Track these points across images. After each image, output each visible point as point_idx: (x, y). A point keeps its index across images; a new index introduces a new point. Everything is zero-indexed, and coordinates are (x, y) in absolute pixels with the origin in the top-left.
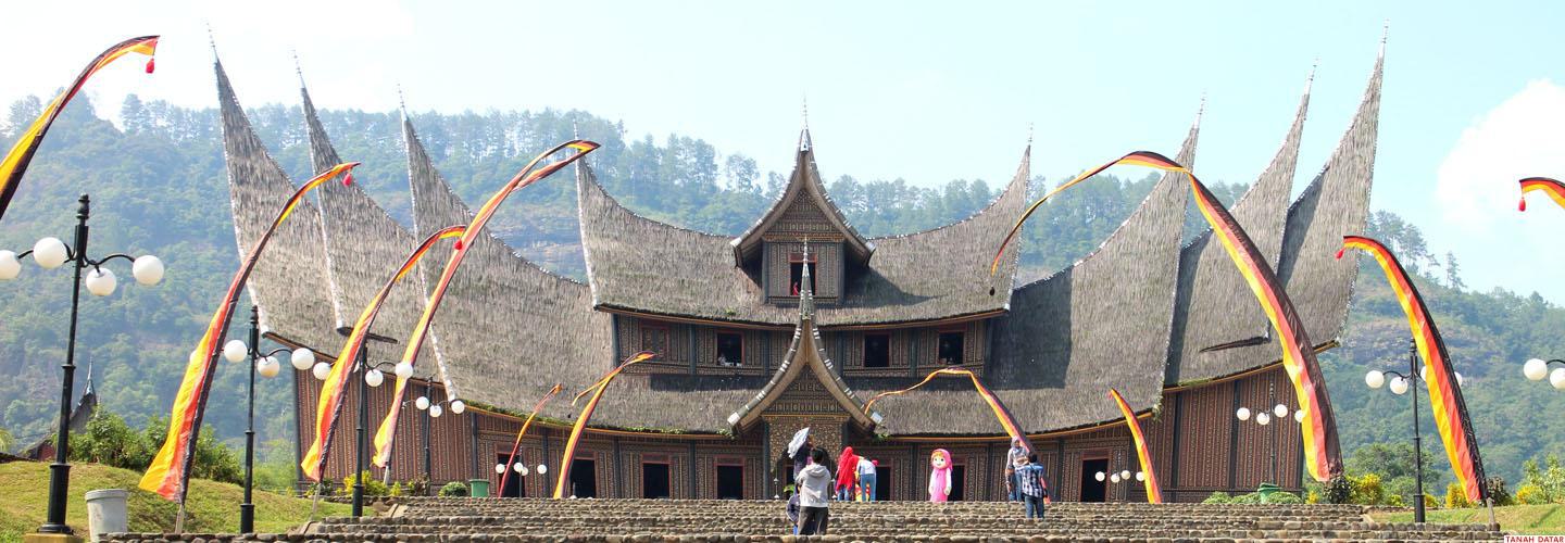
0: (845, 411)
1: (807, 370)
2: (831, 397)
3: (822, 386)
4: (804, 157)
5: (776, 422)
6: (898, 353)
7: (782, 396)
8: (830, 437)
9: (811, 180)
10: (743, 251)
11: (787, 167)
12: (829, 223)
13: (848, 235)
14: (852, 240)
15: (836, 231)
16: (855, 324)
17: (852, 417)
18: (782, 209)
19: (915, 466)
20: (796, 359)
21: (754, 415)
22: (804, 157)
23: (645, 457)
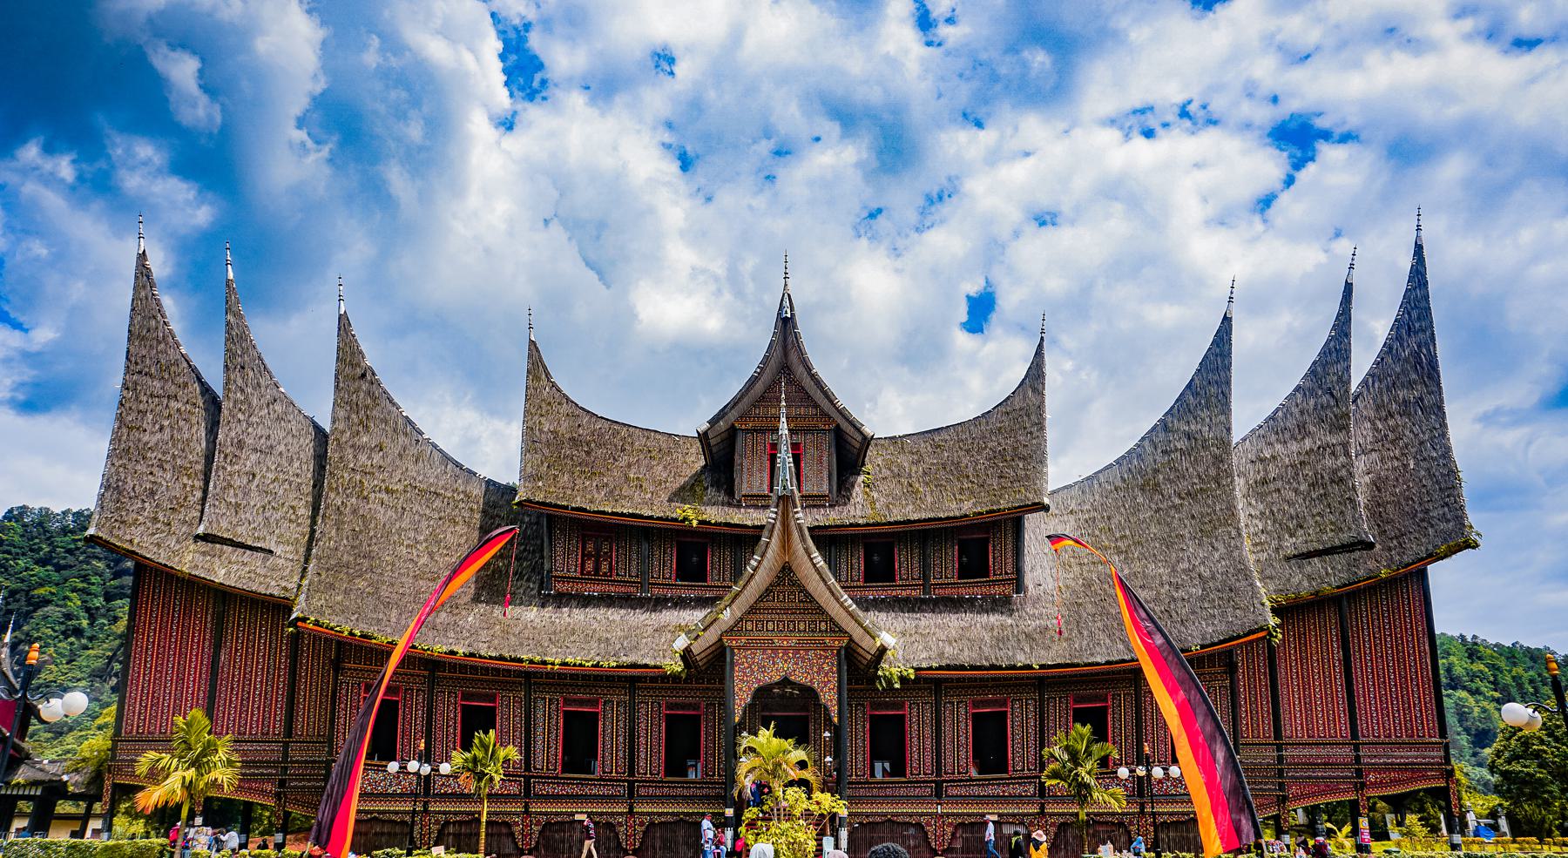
0: (842, 630)
1: (786, 572)
2: (821, 611)
3: (808, 595)
4: (786, 325)
5: (745, 648)
6: (906, 563)
7: (752, 610)
8: (820, 669)
9: (793, 357)
10: (713, 442)
11: (761, 337)
12: (816, 406)
13: (840, 420)
14: (845, 426)
15: (825, 415)
16: (851, 525)
17: (851, 640)
18: (759, 387)
19: (938, 711)
20: (770, 553)
21: (711, 637)
22: (786, 325)
23: (567, 702)
